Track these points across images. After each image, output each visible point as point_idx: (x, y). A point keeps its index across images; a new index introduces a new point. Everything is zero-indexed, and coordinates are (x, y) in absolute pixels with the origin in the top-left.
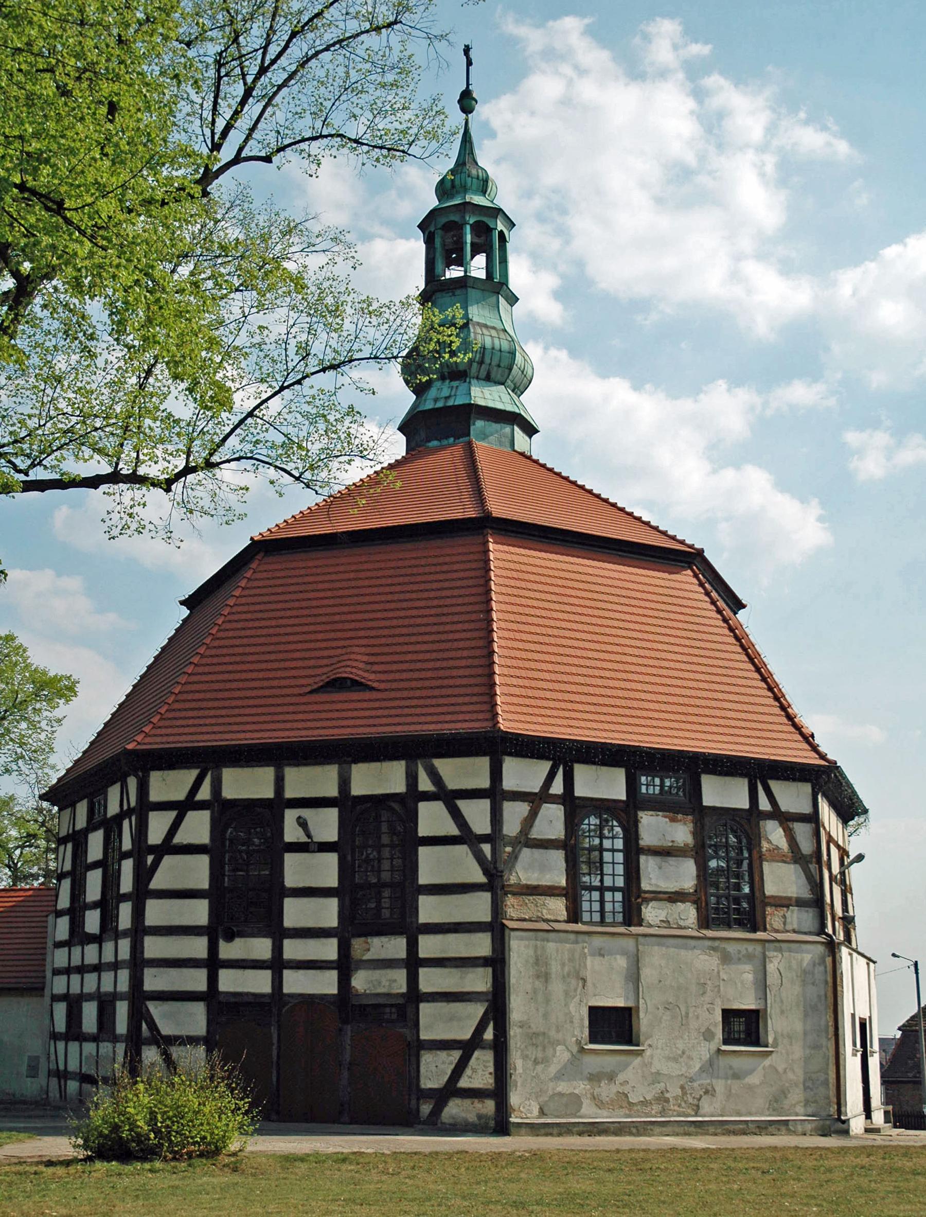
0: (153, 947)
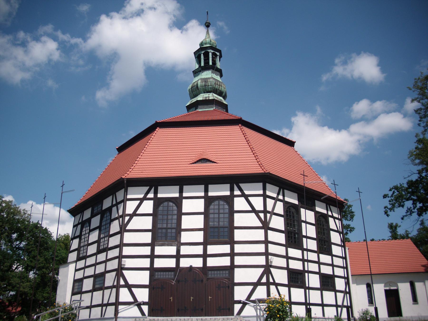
0: (127, 251)
